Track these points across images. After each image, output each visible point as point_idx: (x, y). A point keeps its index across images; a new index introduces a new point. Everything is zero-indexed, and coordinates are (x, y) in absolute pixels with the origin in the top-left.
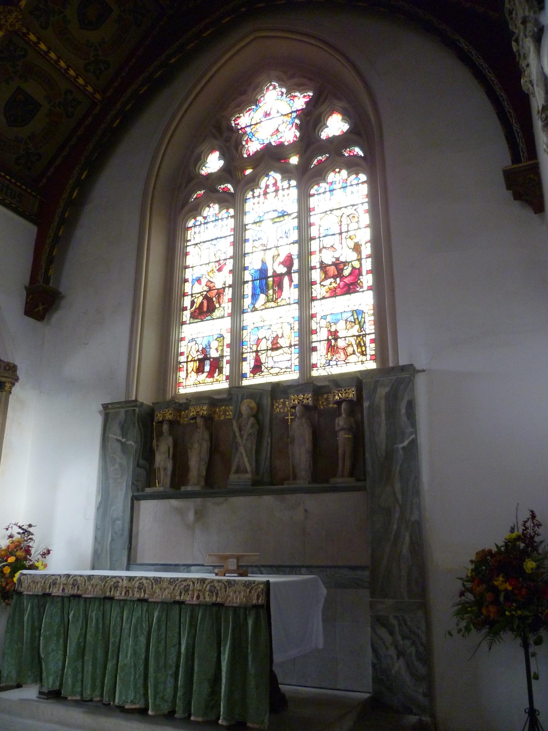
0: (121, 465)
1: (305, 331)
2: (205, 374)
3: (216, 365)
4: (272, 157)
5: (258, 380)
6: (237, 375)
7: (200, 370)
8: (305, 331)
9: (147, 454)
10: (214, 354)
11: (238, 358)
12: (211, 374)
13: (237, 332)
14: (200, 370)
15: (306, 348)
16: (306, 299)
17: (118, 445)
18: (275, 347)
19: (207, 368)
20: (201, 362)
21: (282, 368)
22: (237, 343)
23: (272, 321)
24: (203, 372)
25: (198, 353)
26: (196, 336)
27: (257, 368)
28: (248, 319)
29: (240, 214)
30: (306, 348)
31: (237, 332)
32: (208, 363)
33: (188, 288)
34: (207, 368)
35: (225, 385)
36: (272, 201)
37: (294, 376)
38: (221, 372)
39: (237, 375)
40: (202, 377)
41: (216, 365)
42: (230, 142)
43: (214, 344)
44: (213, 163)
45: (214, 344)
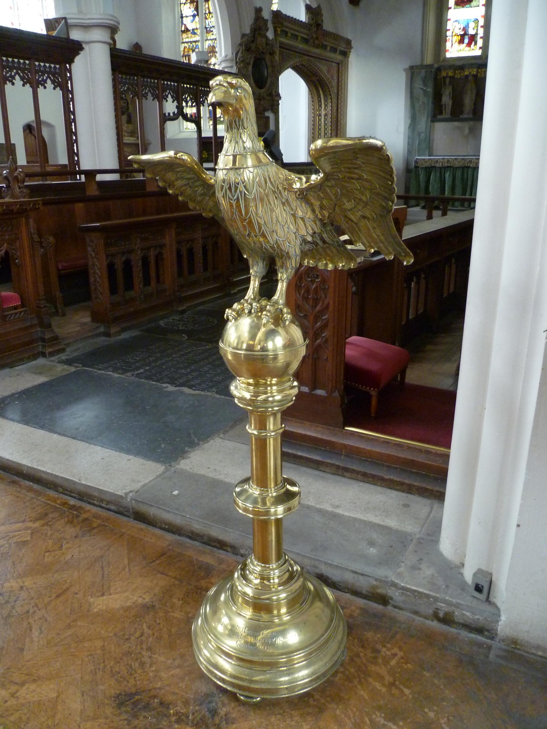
0: (424, 103)
2: (465, 45)
3: (473, 39)
7: (461, 41)
9: (437, 96)
10: (471, 32)
12: (469, 45)
14: (461, 41)
17: (421, 91)
19: (466, 41)
20: (462, 37)
24: (463, 43)
25: (461, 30)
34: (466, 41)
38: (476, 44)
40: (463, 46)
41: (473, 39)
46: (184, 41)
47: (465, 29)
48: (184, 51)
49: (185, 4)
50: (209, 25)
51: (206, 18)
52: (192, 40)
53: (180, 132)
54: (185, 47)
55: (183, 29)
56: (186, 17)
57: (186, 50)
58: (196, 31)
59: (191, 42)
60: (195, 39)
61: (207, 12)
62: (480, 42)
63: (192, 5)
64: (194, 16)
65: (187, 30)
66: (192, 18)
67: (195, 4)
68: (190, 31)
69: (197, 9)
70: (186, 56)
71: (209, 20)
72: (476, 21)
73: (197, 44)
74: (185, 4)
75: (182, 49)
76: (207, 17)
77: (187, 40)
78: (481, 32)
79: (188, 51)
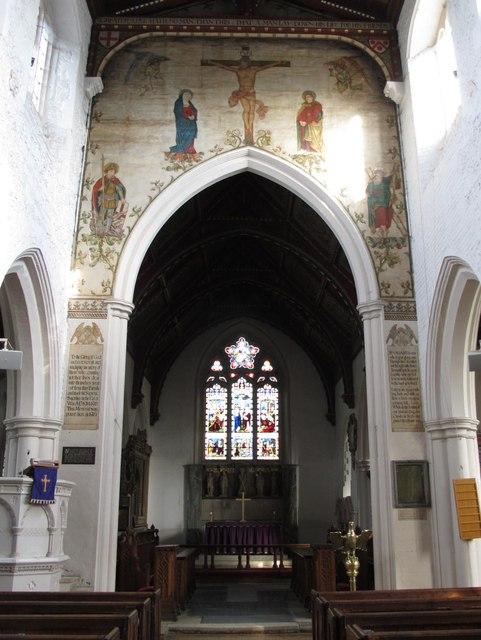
1: (255, 443)
3: (221, 450)
4: (242, 372)
5: (237, 458)
6: (229, 455)
7: (214, 451)
8: (255, 443)
10: (220, 446)
11: (229, 449)
12: (219, 453)
13: (229, 438)
15: (255, 449)
16: (255, 432)
18: (244, 447)
21: (246, 455)
22: (229, 443)
23: (243, 437)
26: (211, 438)
27: (237, 454)
28: (233, 435)
29: (229, 392)
30: (255, 449)
31: (229, 438)
32: (216, 449)
33: (207, 417)
35: (225, 458)
36: (242, 389)
37: (251, 458)
39: (229, 455)
41: (221, 450)
42: (226, 360)
43: (220, 442)
44: (217, 366)
45: (220, 442)
47: (216, 444)
62: (225, 453)
72: (222, 440)
78: (225, 446)
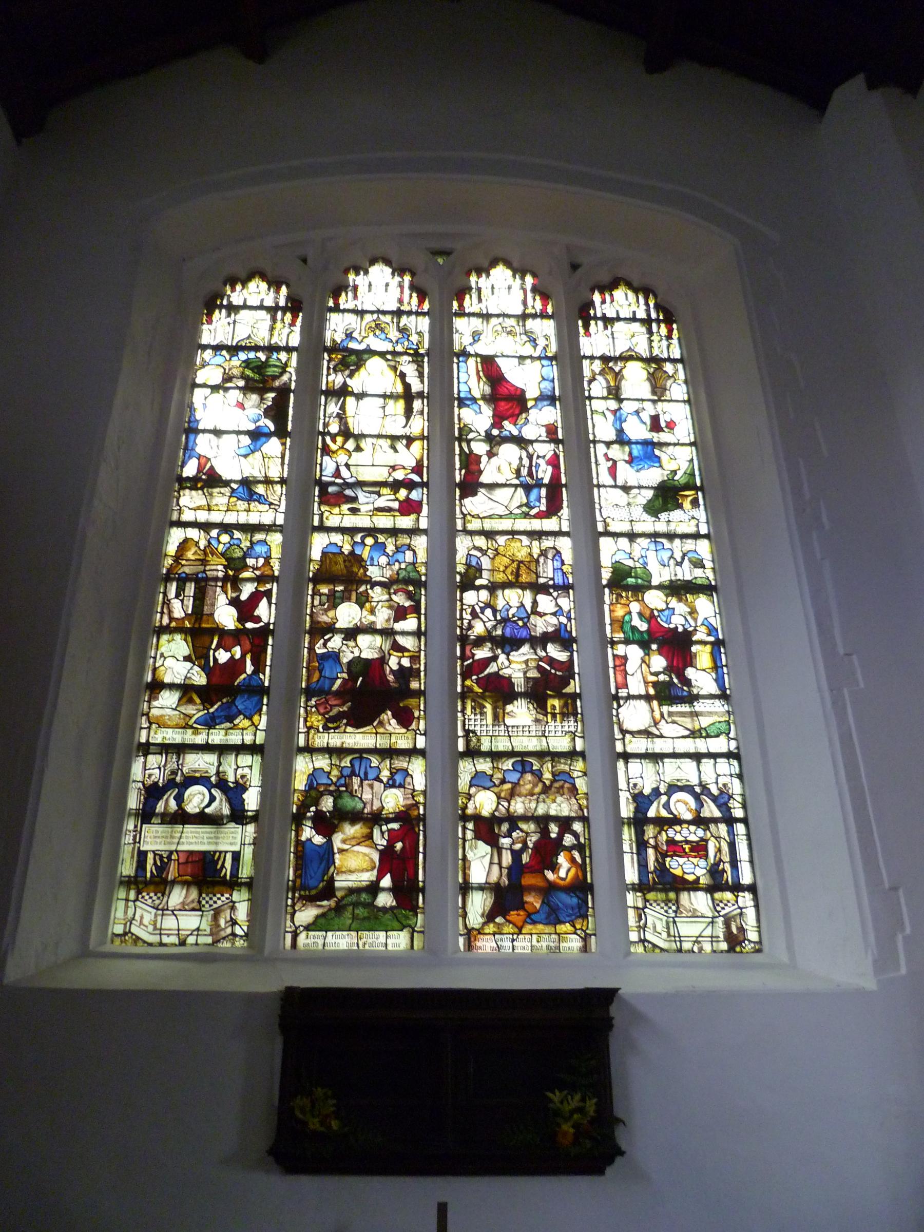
46: (187, 516)
48: (178, 557)
49: (215, 388)
50: (337, 474)
51: (326, 451)
52: (231, 518)
53: (85, 953)
54: (184, 545)
55: (190, 470)
56: (217, 433)
57: (190, 555)
58: (260, 489)
59: (226, 528)
60: (253, 519)
61: (334, 428)
63: (255, 398)
64: (257, 435)
65: (209, 480)
66: (246, 440)
67: (271, 395)
68: (226, 483)
69: (277, 412)
70: (182, 582)
71: (342, 458)
73: (259, 536)
74: (215, 388)
75: (172, 549)
76: (333, 447)
77: (202, 517)
79: (204, 562)
